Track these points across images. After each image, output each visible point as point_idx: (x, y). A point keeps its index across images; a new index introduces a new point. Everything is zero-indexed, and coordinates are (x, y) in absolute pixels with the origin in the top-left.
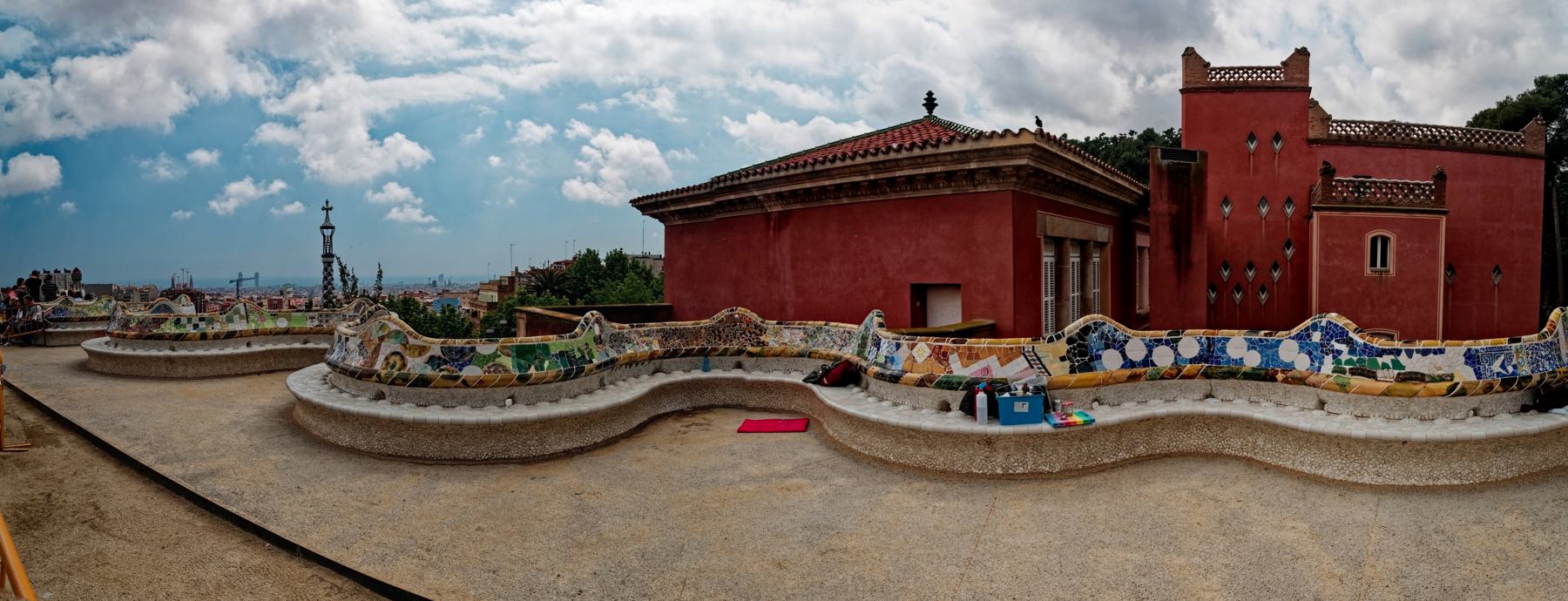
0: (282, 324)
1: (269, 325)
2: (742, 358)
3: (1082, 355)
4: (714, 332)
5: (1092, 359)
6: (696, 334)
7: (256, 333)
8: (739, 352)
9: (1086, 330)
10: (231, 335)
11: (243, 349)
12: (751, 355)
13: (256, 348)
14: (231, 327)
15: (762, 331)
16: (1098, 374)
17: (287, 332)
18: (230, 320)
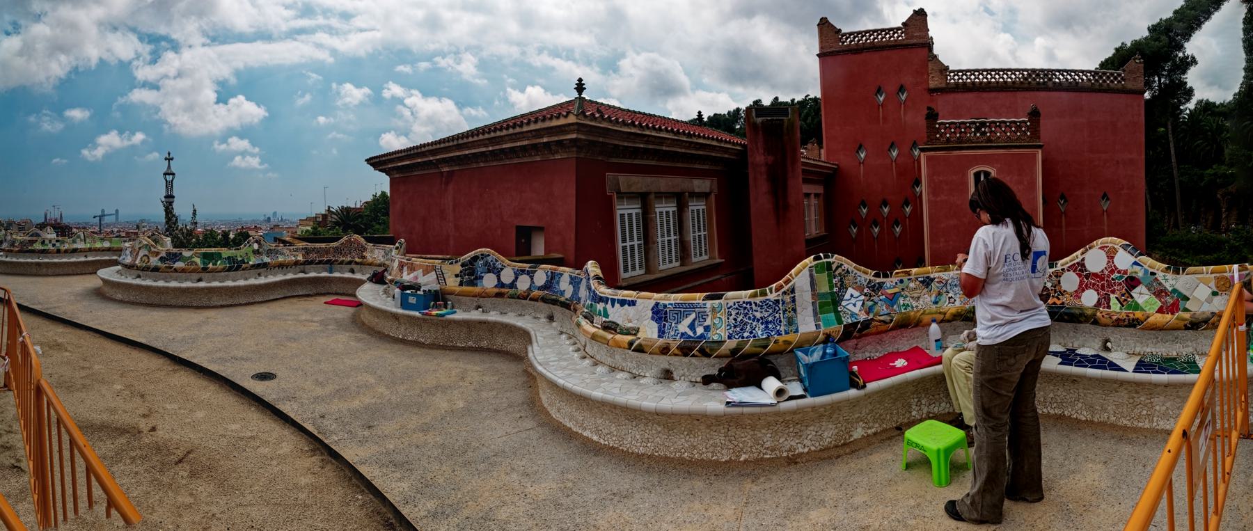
0: (107, 245)
1: (98, 245)
2: (353, 266)
3: (470, 275)
4: (337, 250)
5: (476, 278)
6: (327, 251)
7: (90, 250)
8: (350, 263)
9: (475, 258)
10: (75, 251)
11: (83, 259)
12: (357, 263)
13: (90, 259)
14: (75, 246)
15: (365, 249)
16: (477, 289)
17: (109, 250)
18: (74, 242)
